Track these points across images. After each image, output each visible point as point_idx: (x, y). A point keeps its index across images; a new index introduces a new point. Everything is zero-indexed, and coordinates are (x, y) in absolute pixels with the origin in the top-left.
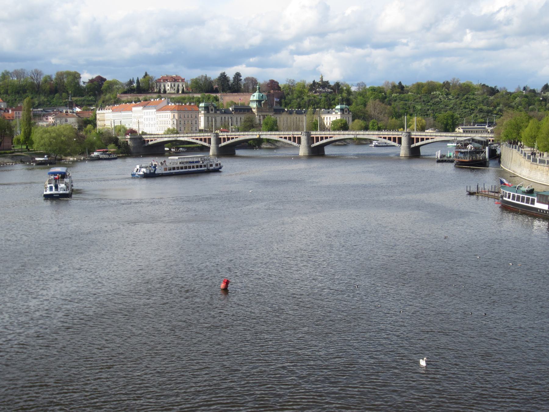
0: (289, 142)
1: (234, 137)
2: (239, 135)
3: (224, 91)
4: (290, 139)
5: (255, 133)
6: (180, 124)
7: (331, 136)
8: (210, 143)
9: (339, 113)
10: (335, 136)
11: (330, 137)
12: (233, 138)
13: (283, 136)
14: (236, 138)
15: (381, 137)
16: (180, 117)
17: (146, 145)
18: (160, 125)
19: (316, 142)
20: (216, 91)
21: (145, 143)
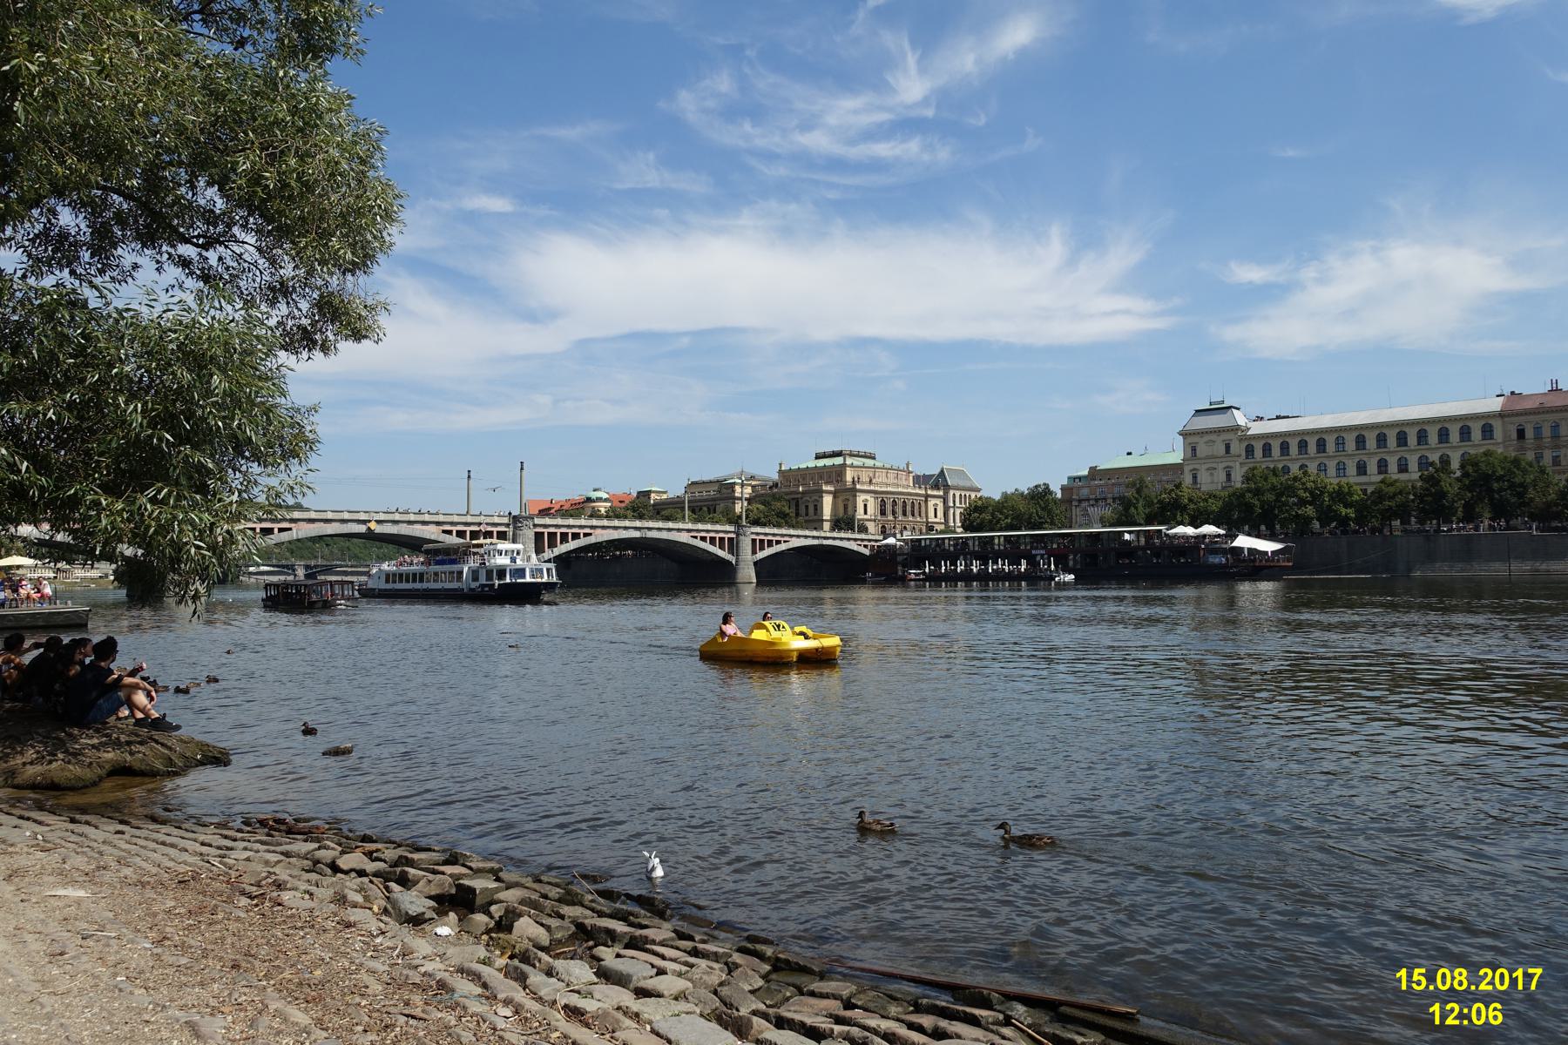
7: (587, 531)
10: (599, 531)
11: (586, 535)
13: (454, 529)
14: (281, 530)
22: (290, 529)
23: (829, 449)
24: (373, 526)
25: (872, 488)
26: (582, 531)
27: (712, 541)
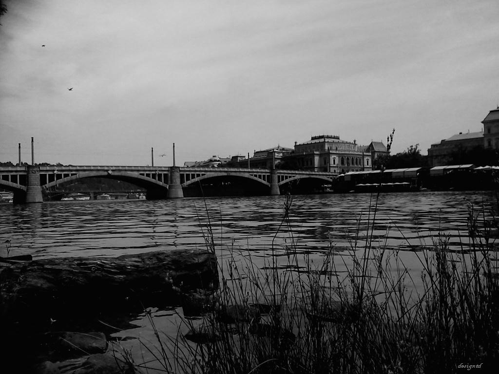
7: (203, 173)
10: (208, 173)
12: (66, 176)
13: (145, 173)
22: (76, 174)
23: (317, 135)
24: (110, 172)
25: (337, 152)
26: (201, 173)
27: (260, 177)
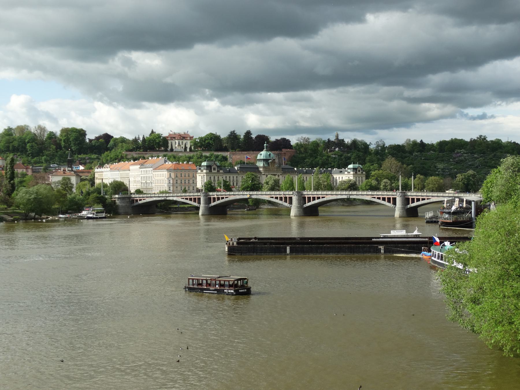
0: (280, 202)
1: (225, 196)
2: (229, 195)
3: (233, 148)
4: (281, 199)
5: (246, 193)
6: (177, 183)
8: (199, 203)
9: (352, 173)
11: (322, 197)
12: (222, 198)
14: (226, 198)
15: (375, 198)
16: (177, 176)
17: (135, 204)
18: (156, 185)
19: (308, 202)
20: (226, 150)
21: (134, 203)
22: (228, 197)
